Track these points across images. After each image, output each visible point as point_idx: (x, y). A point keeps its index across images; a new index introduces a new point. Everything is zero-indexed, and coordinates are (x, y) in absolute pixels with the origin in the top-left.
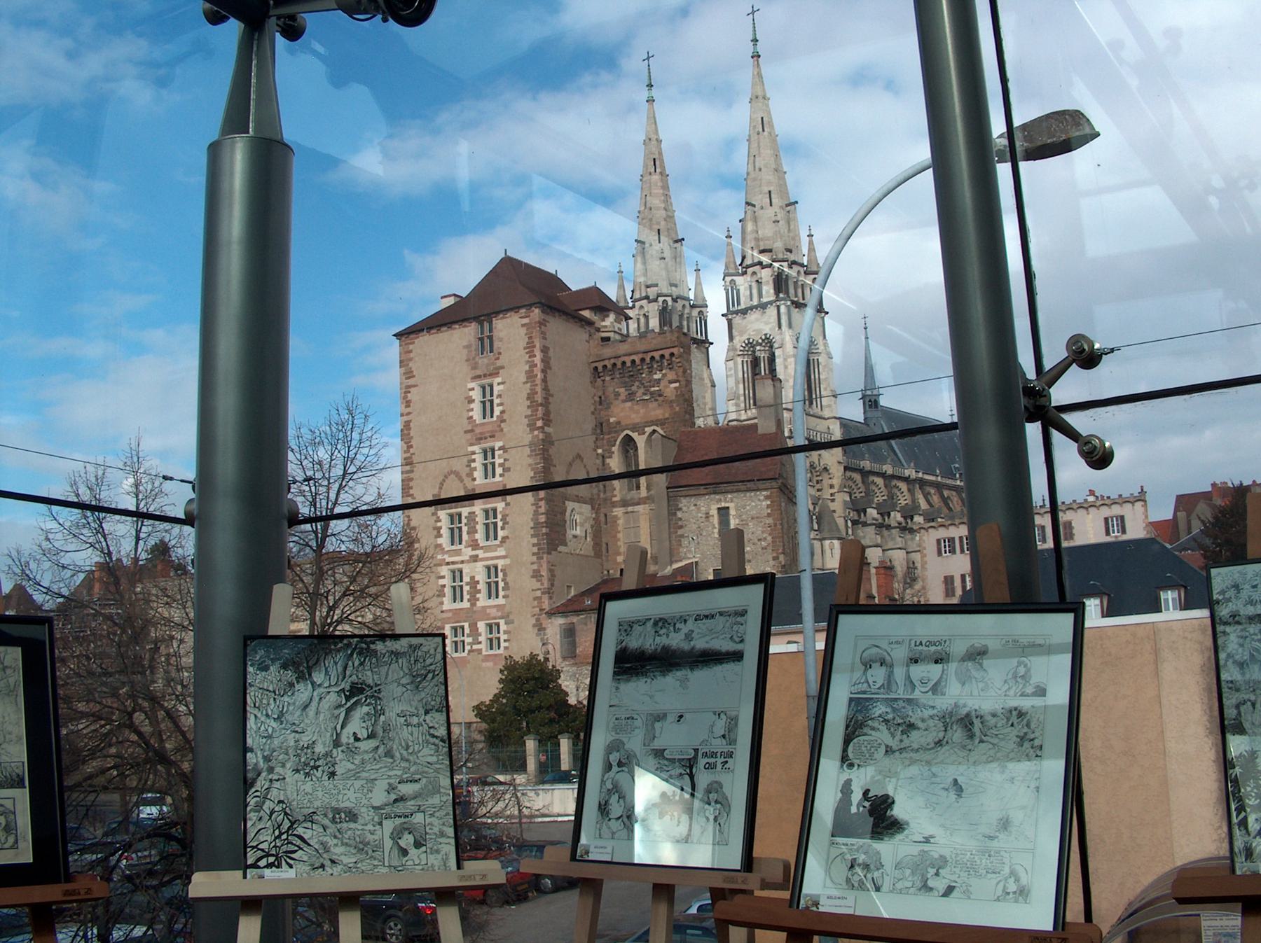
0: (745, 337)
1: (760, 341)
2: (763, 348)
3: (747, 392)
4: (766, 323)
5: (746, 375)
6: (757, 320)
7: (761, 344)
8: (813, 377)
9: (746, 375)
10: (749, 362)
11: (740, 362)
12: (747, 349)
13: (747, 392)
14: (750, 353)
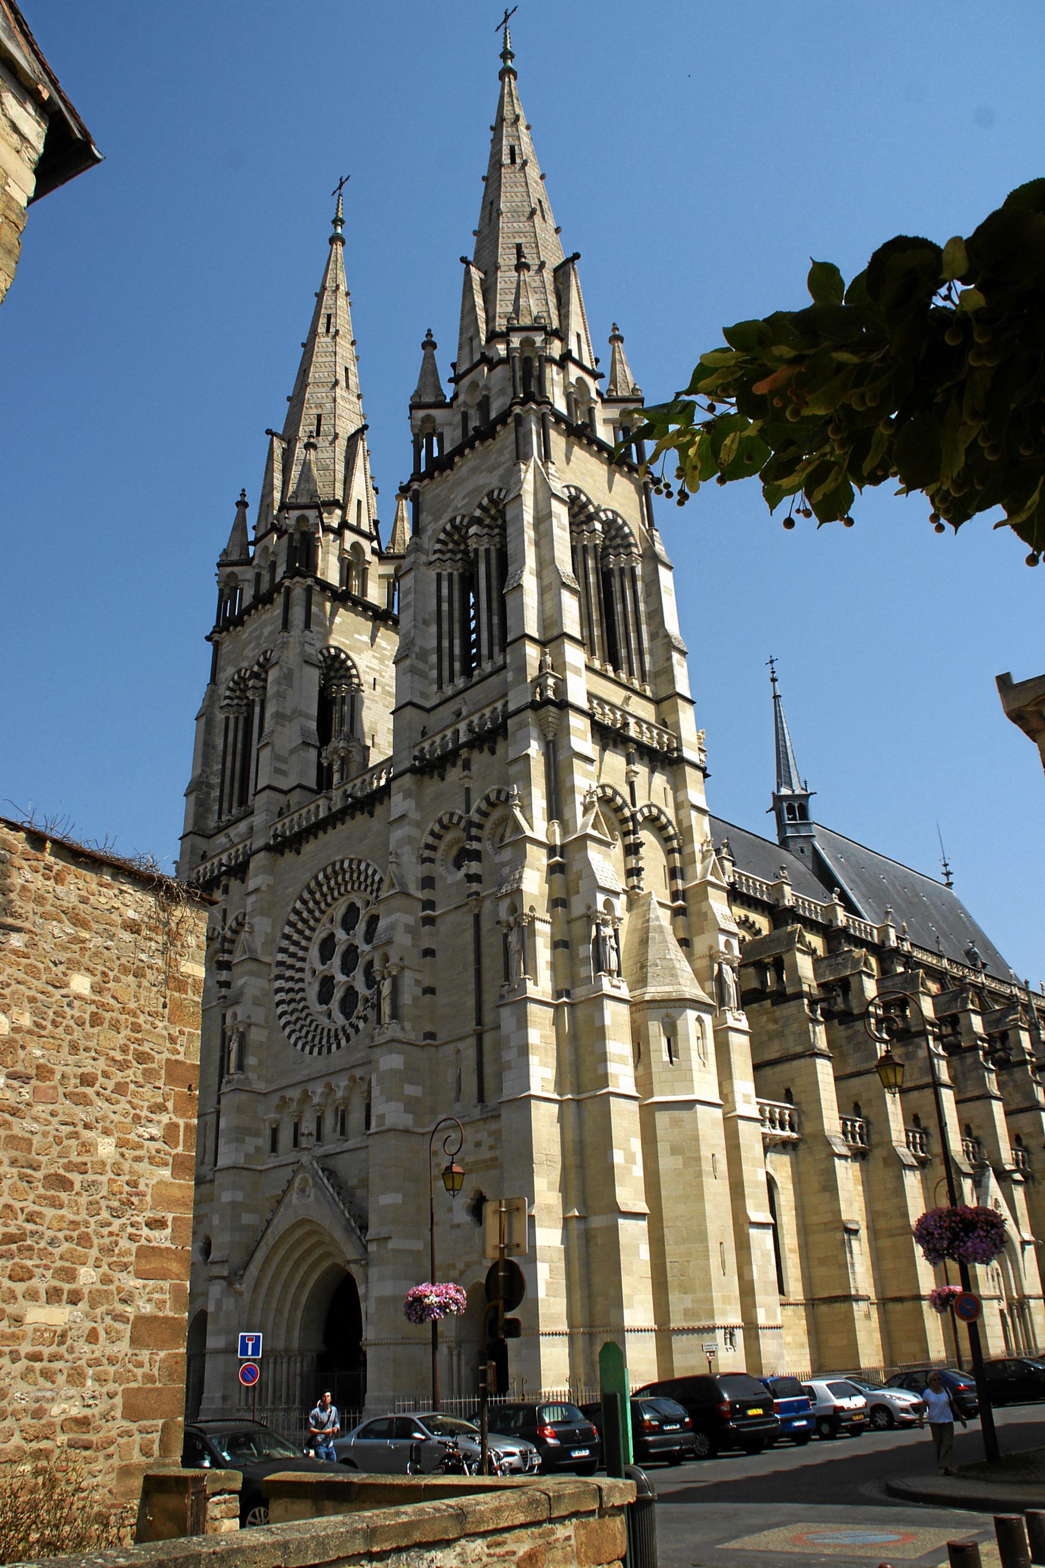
0: (444, 521)
1: (478, 513)
2: (486, 530)
3: (446, 643)
4: (490, 470)
5: (445, 606)
6: (474, 471)
7: (479, 521)
8: (619, 608)
9: (445, 606)
10: (456, 578)
11: (433, 574)
12: (451, 546)
13: (446, 643)
14: (459, 556)
